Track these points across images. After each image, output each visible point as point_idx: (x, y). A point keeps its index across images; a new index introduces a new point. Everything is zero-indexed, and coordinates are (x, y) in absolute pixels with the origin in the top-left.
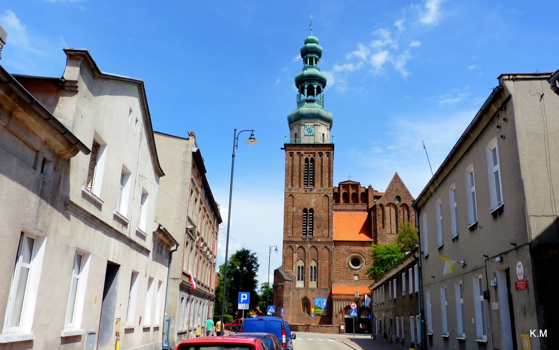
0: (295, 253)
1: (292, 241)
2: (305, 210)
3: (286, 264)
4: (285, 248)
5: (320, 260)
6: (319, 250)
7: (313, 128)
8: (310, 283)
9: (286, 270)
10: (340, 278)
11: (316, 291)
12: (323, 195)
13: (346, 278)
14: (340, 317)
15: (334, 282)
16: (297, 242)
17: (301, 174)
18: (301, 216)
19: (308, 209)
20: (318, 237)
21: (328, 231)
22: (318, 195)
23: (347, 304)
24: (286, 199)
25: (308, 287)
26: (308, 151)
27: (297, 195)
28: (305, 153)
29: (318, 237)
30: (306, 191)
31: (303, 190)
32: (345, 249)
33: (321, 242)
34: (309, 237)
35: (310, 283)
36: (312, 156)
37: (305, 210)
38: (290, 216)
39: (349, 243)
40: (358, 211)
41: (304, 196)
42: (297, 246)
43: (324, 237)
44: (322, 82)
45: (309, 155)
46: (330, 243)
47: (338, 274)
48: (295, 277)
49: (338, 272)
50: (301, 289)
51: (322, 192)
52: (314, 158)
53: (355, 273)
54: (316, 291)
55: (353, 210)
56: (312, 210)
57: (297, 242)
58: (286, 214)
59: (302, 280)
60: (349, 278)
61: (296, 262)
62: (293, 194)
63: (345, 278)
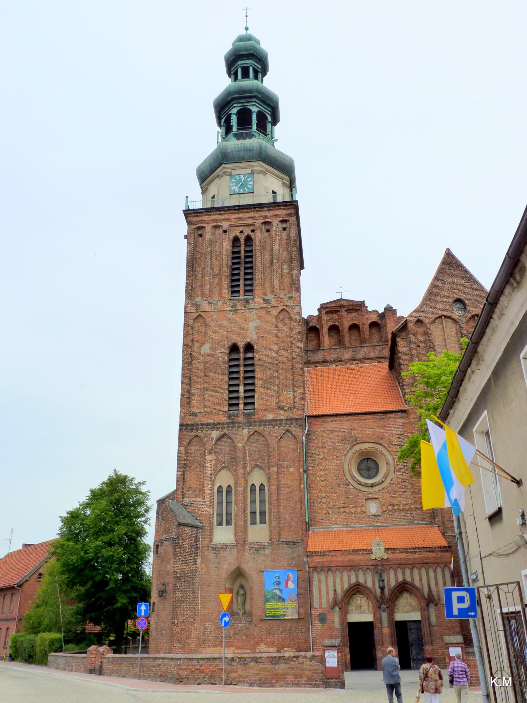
0: (210, 453)
1: (203, 425)
2: (234, 348)
3: (188, 484)
4: (185, 443)
5: (274, 466)
6: (273, 441)
7: (250, 179)
8: (251, 528)
9: (186, 500)
10: (330, 511)
11: (266, 550)
12: (275, 312)
13: (347, 510)
14: (333, 622)
15: (313, 522)
16: (214, 426)
17: (224, 269)
18: (224, 363)
19: (241, 346)
20: (266, 409)
21: (292, 393)
22: (264, 312)
23: (353, 581)
24: (188, 326)
25: (245, 541)
26: (239, 222)
27: (215, 316)
28: (231, 226)
29: (266, 409)
30: (235, 306)
31: (228, 303)
32: (337, 436)
33: (275, 420)
34: (246, 411)
35: (251, 528)
36: (247, 231)
37: (234, 348)
38: (198, 365)
39: (348, 420)
40: (366, 361)
41: (229, 316)
42: (215, 434)
43: (282, 408)
44: (269, 105)
45: (241, 229)
46: (300, 422)
47: (324, 500)
48: (211, 517)
49: (323, 495)
50: (226, 547)
51: (274, 304)
52: (252, 235)
53: (370, 496)
54: (268, 551)
55: (355, 360)
56: (249, 347)
57: (214, 426)
58: (186, 360)
59: (228, 523)
60: (353, 510)
61: (213, 477)
62: (203, 314)
63: (342, 510)
